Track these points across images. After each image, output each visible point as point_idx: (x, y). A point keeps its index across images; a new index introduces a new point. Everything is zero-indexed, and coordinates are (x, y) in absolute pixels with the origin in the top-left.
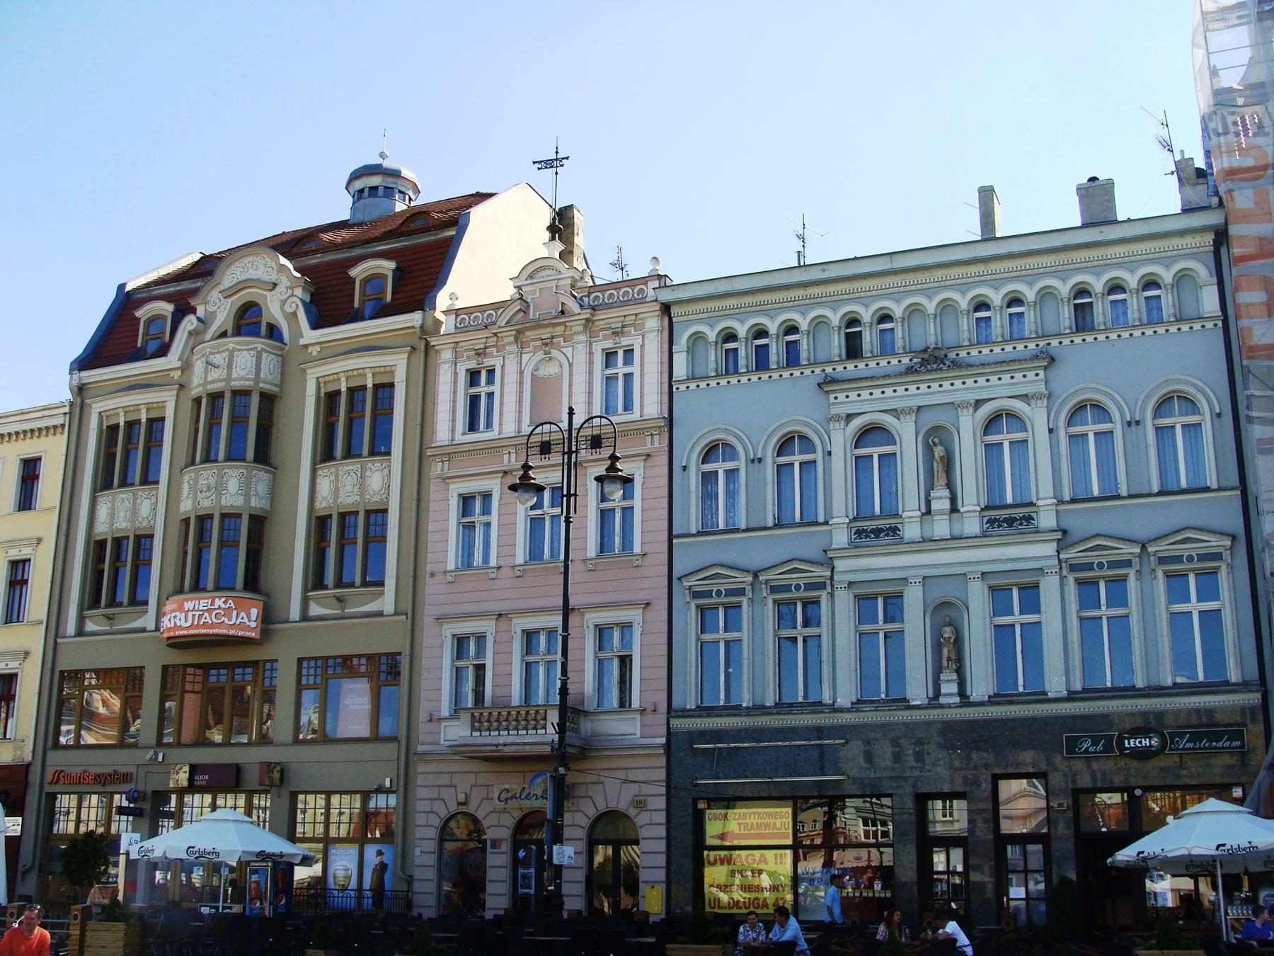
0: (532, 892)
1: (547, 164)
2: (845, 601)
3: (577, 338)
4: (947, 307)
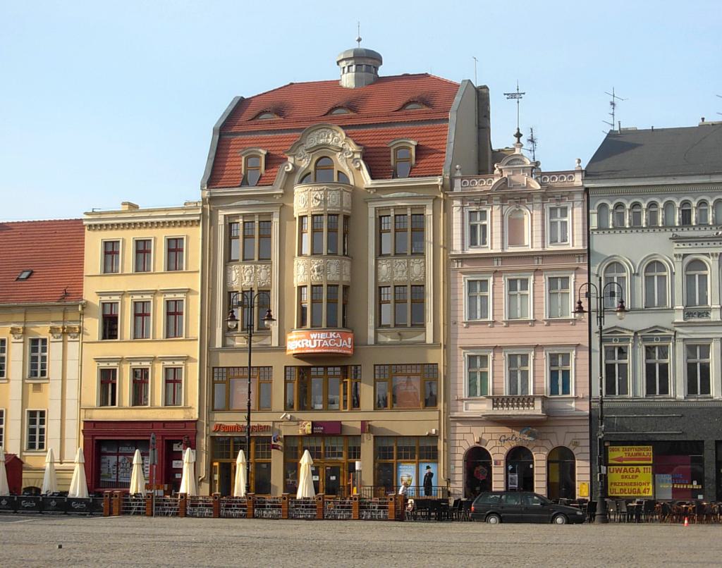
0: (516, 486)
1: (512, 96)
2: (680, 347)
3: (535, 201)
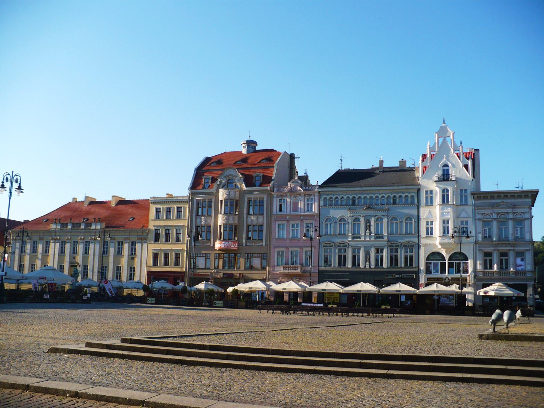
4: (371, 197)
